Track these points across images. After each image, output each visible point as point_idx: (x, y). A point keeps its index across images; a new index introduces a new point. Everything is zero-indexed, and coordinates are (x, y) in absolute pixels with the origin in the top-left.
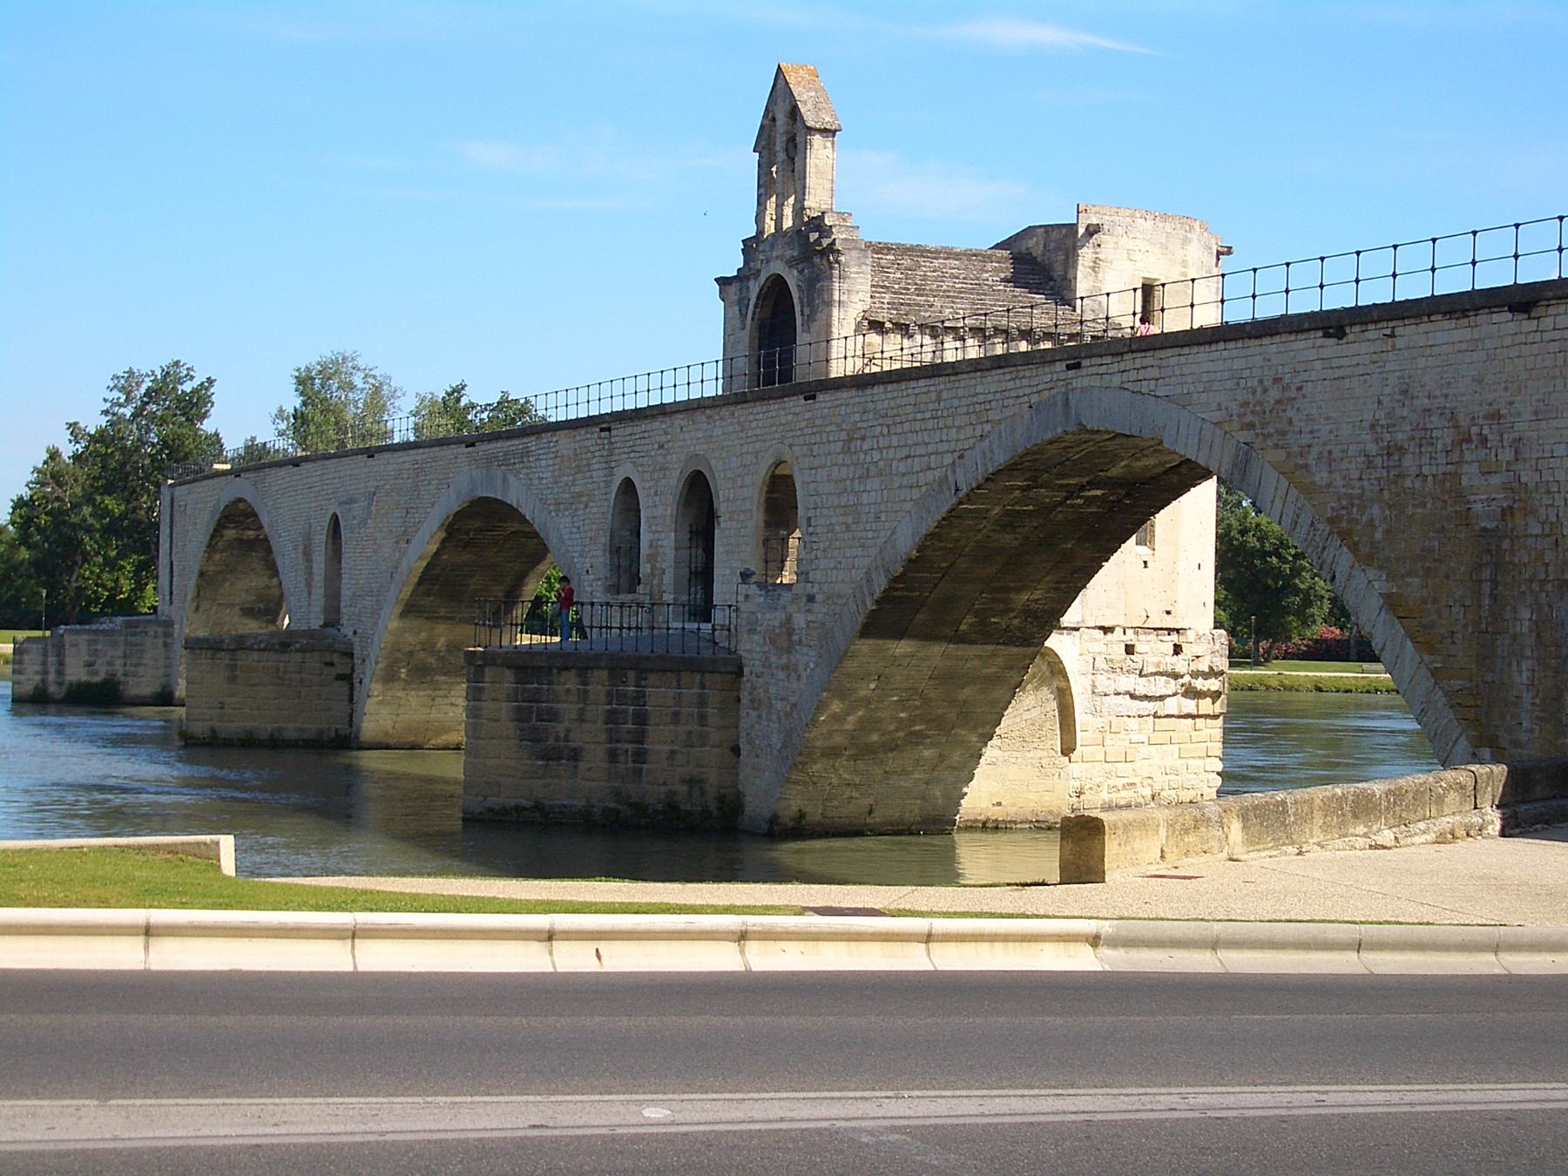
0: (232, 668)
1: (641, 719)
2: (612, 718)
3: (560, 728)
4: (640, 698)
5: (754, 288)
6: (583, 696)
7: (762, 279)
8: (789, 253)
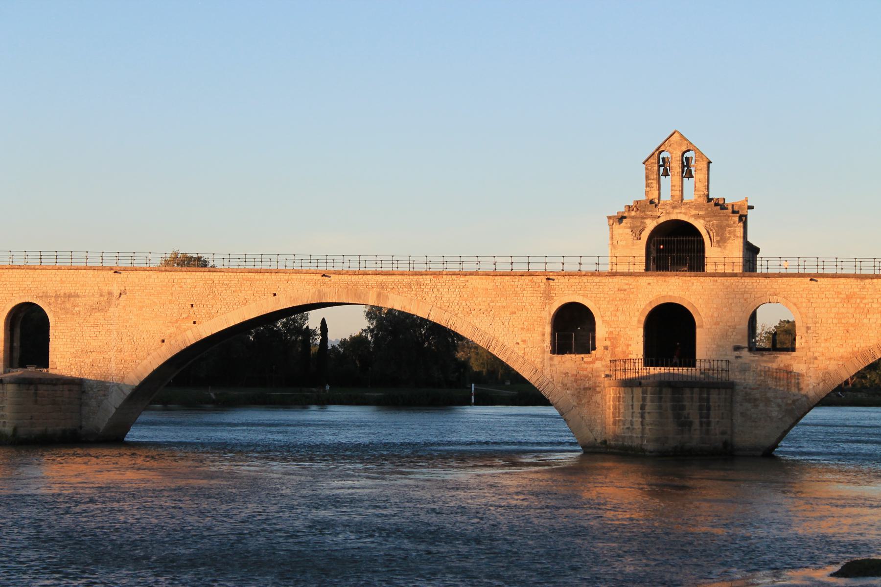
0: (36, 394)
1: (709, 409)
2: (701, 408)
3: (686, 412)
4: (708, 399)
5: (651, 225)
6: (692, 398)
8: (693, 212)
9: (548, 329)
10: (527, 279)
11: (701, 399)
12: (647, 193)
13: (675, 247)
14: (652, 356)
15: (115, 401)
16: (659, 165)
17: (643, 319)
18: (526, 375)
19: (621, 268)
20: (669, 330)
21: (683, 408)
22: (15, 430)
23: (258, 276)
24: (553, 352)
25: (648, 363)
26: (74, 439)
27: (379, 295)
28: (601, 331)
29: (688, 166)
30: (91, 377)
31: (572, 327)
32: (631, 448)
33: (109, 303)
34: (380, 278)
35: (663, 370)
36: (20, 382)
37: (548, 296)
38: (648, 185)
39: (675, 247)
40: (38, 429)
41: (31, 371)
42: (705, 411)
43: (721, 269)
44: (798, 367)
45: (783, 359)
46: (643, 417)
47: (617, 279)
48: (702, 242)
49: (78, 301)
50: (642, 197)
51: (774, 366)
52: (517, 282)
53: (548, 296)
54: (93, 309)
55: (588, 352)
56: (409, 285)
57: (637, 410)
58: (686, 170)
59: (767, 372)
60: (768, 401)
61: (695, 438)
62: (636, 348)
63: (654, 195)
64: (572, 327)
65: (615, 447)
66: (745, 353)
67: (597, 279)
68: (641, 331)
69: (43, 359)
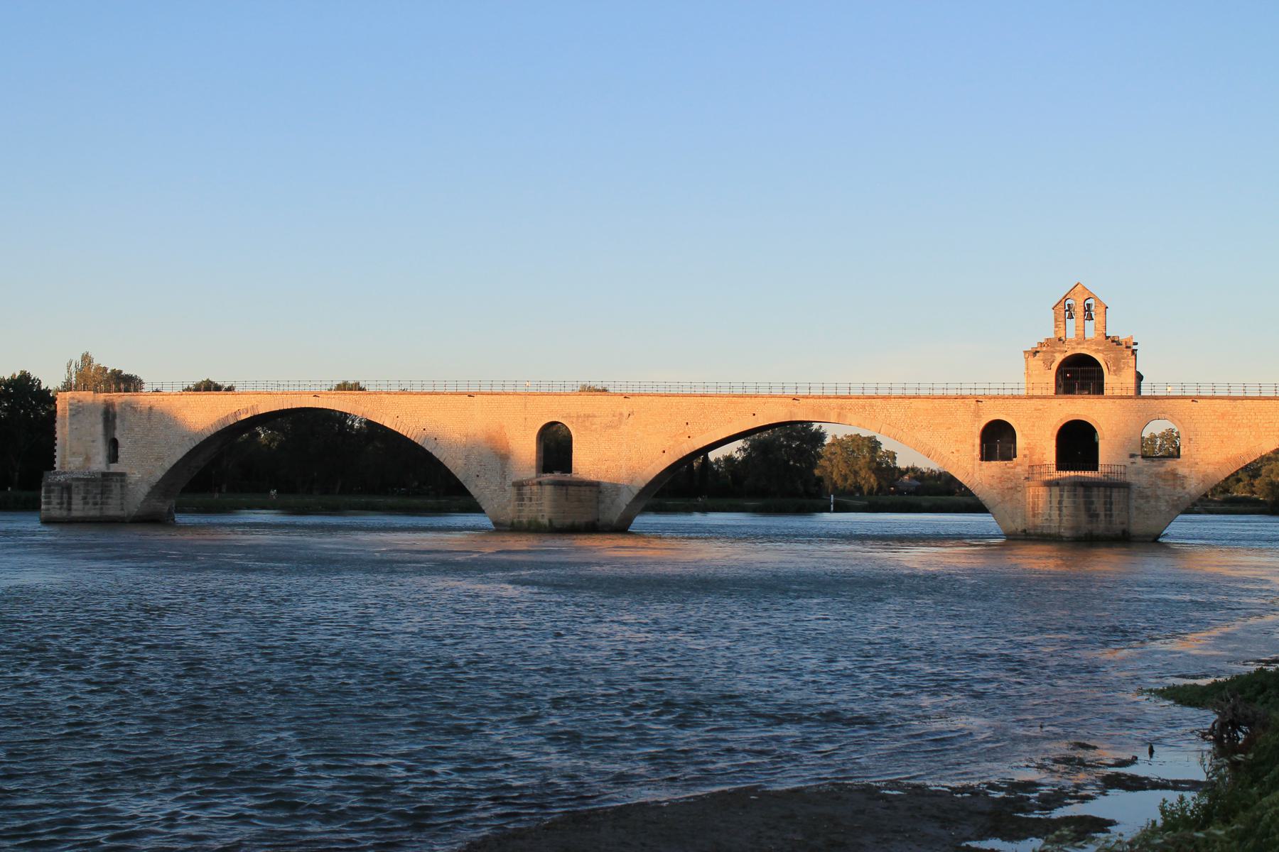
1: (1111, 503)
2: (1105, 503)
4: (1110, 497)
5: (1059, 358)
7: (1068, 354)
9: (978, 441)
10: (959, 401)
11: (1105, 496)
12: (1056, 332)
13: (1080, 374)
14: (1064, 460)
15: (625, 499)
16: (1065, 310)
17: (1055, 433)
18: (960, 478)
19: (1037, 392)
20: (1077, 442)
21: (1092, 503)
22: (550, 520)
23: (740, 400)
24: (982, 459)
25: (1059, 468)
26: (593, 528)
27: (839, 414)
28: (1021, 442)
29: (1089, 310)
30: (606, 480)
31: (997, 439)
32: (1049, 535)
33: (620, 422)
34: (840, 401)
35: (1072, 473)
36: (557, 484)
37: (977, 414)
38: (1056, 326)
39: (1080, 374)
40: (569, 521)
41: (557, 476)
42: (1109, 504)
43: (1117, 392)
44: (1182, 471)
45: (1170, 464)
46: (1060, 509)
47: (1034, 401)
48: (1102, 371)
49: (595, 420)
50: (1052, 336)
51: (1162, 470)
52: (952, 403)
53: (977, 414)
54: (608, 427)
55: (1010, 459)
56: (864, 407)
57: (1055, 504)
59: (1158, 475)
60: (1157, 498)
61: (1100, 527)
62: (1050, 455)
63: (1061, 334)
64: (997, 439)
65: (1036, 534)
66: (1139, 459)
67: (1017, 401)
68: (1054, 443)
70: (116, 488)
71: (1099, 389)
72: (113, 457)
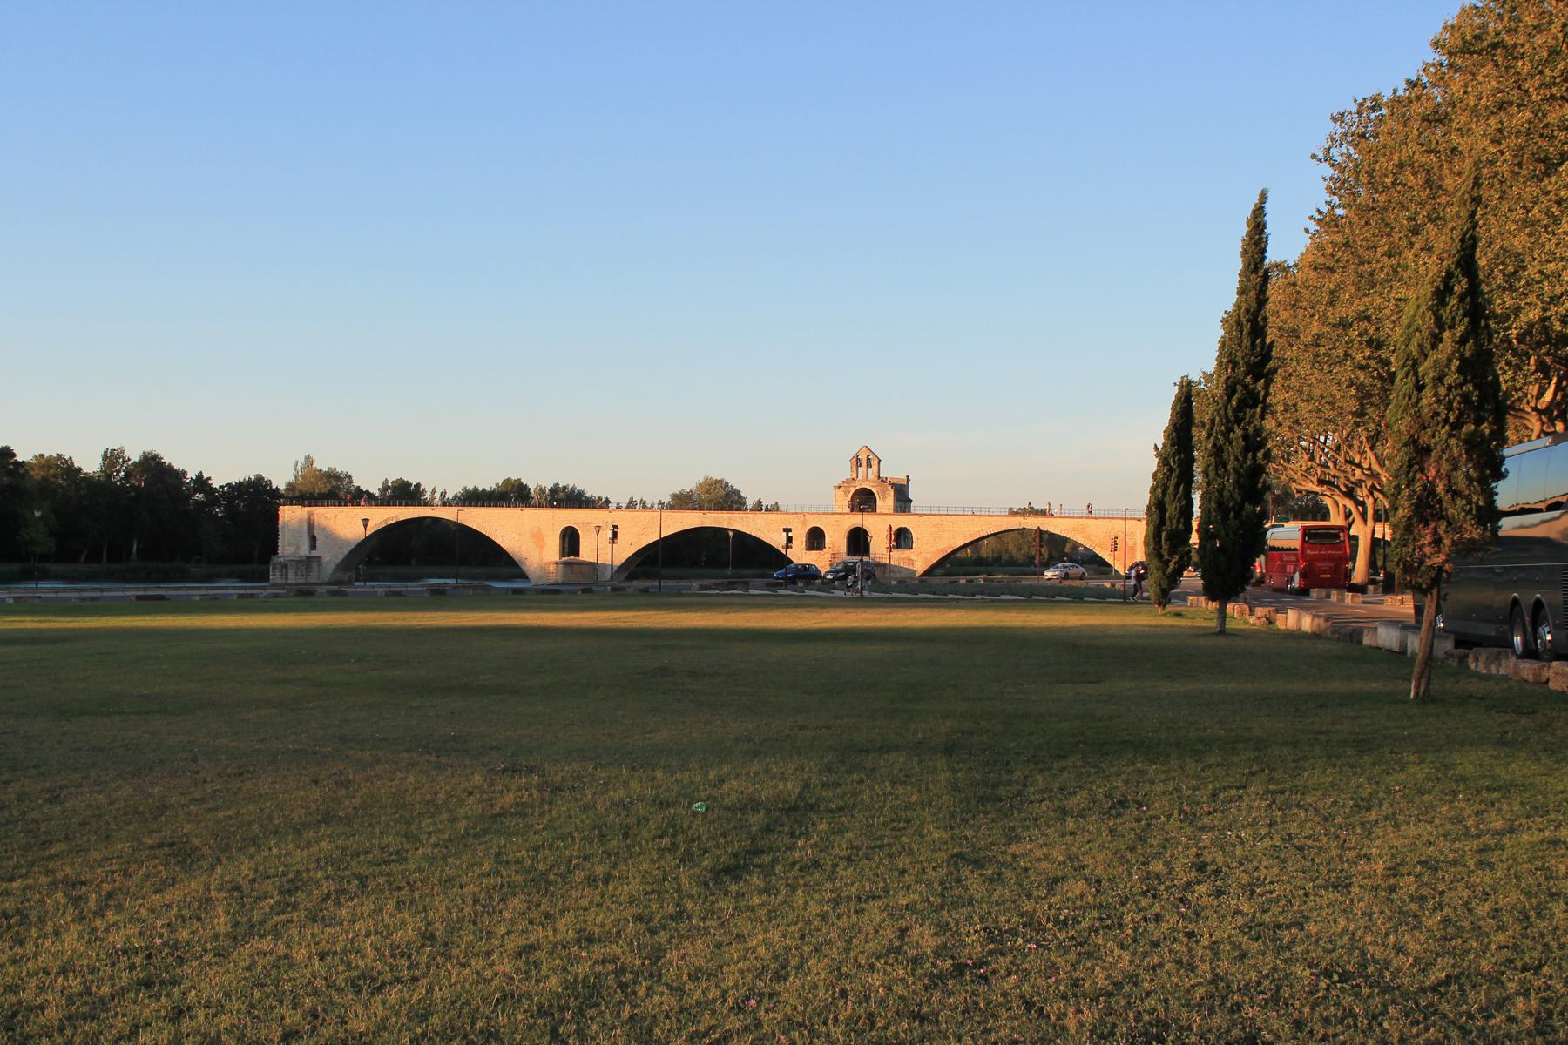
5: (853, 490)
20: (858, 540)
36: (566, 564)
37: (804, 524)
39: (864, 500)
44: (914, 557)
53: (804, 524)
58: (869, 465)
64: (816, 538)
69: (577, 554)
70: (315, 565)
71: (874, 510)
72: (313, 547)
